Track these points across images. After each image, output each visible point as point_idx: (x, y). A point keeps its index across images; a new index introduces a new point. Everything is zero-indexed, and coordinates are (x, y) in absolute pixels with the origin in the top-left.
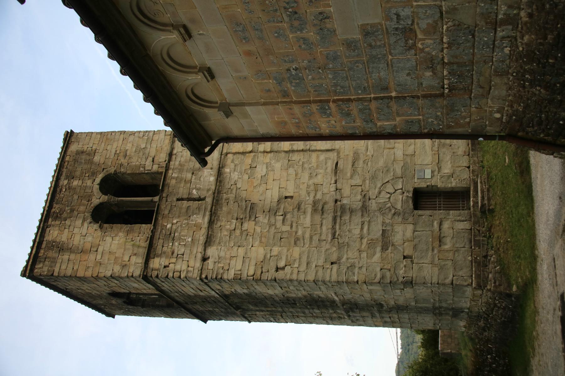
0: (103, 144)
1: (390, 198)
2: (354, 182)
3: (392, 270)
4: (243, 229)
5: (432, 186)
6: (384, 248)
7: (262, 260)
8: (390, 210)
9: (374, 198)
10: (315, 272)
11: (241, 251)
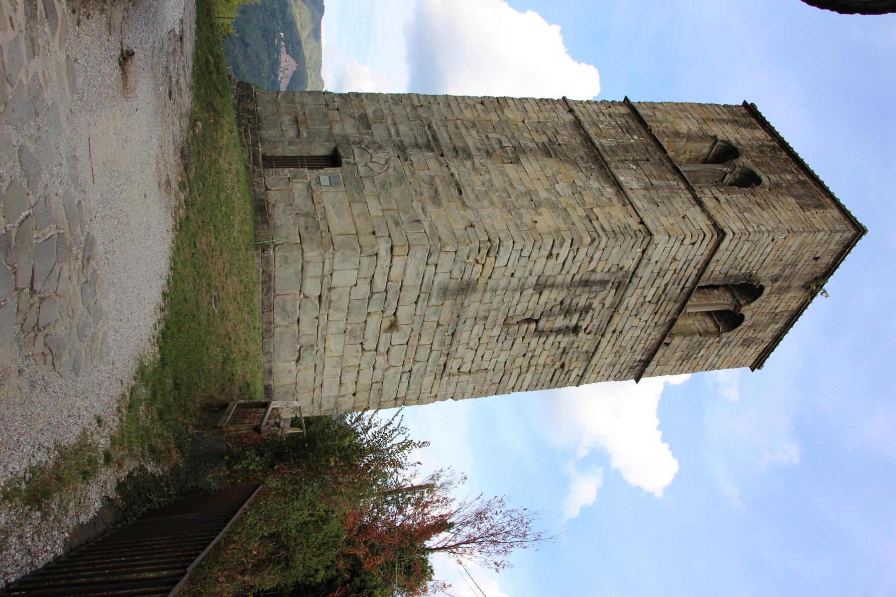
8: (367, 146)
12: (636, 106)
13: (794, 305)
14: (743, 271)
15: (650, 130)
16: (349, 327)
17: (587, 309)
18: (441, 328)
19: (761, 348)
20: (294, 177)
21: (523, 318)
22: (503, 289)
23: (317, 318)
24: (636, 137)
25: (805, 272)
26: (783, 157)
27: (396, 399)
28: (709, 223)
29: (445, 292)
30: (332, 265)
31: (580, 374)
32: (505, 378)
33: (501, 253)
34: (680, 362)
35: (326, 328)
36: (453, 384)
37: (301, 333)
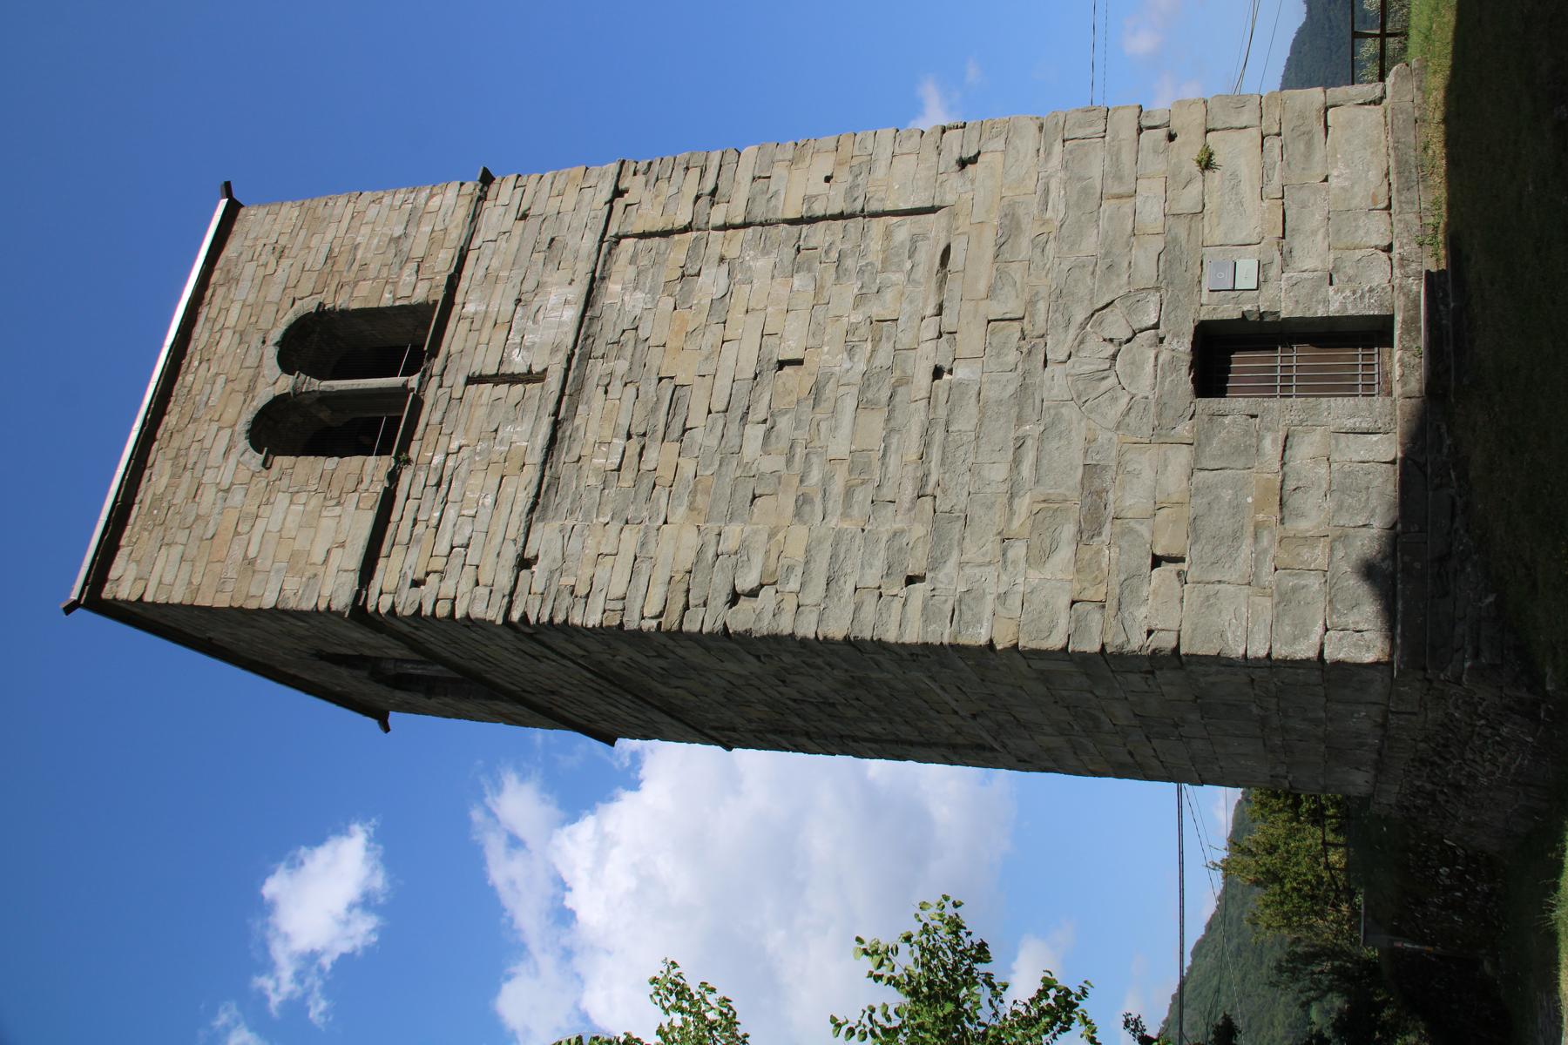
0: (303, 233)
1: (1114, 357)
2: (996, 310)
3: (1112, 604)
4: (644, 467)
5: (1262, 315)
6: (1090, 527)
7: (688, 566)
9: (1063, 358)
10: (852, 607)
11: (631, 538)
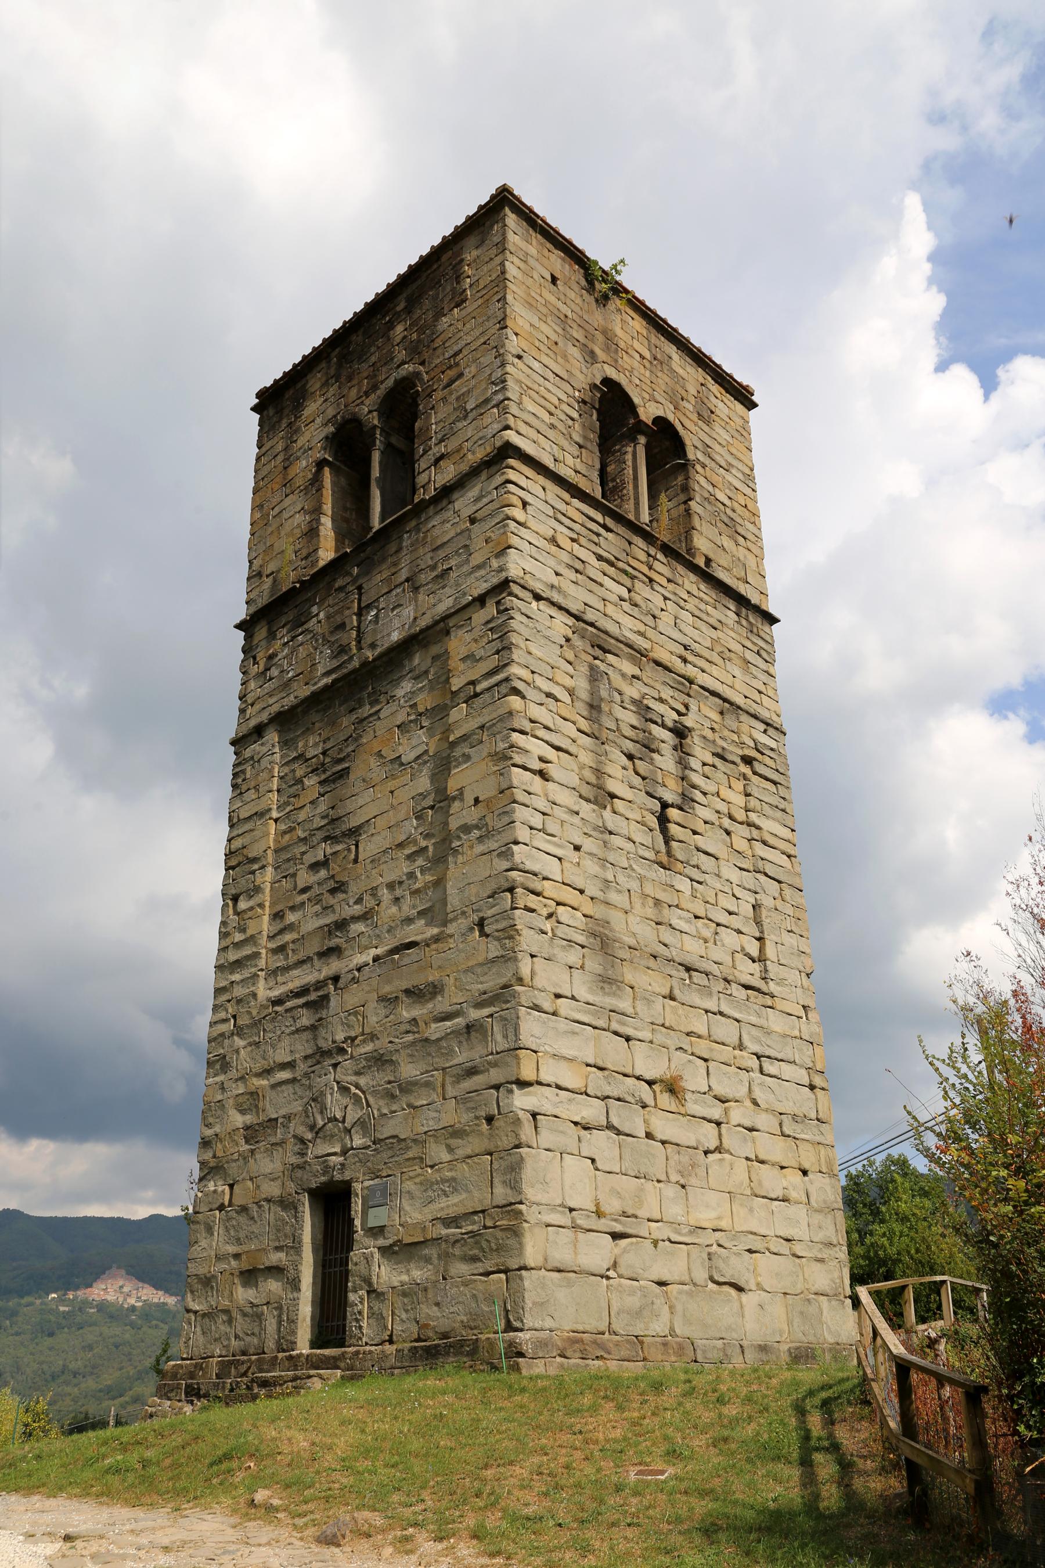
1: (336, 1120)
12: (253, 609)
13: (638, 324)
14: (575, 415)
15: (302, 582)
16: (674, 1177)
17: (642, 709)
18: (677, 992)
19: (715, 388)
20: (368, 1281)
21: (657, 832)
22: (603, 867)
23: (655, 1243)
24: (315, 609)
25: (579, 301)
26: (360, 338)
27: (812, 1087)
28: (484, 475)
29: (607, 982)
30: (552, 1208)
31: (762, 727)
32: (770, 869)
33: (535, 868)
34: (741, 540)
35: (674, 1224)
36: (783, 972)
37: (686, 1278)
